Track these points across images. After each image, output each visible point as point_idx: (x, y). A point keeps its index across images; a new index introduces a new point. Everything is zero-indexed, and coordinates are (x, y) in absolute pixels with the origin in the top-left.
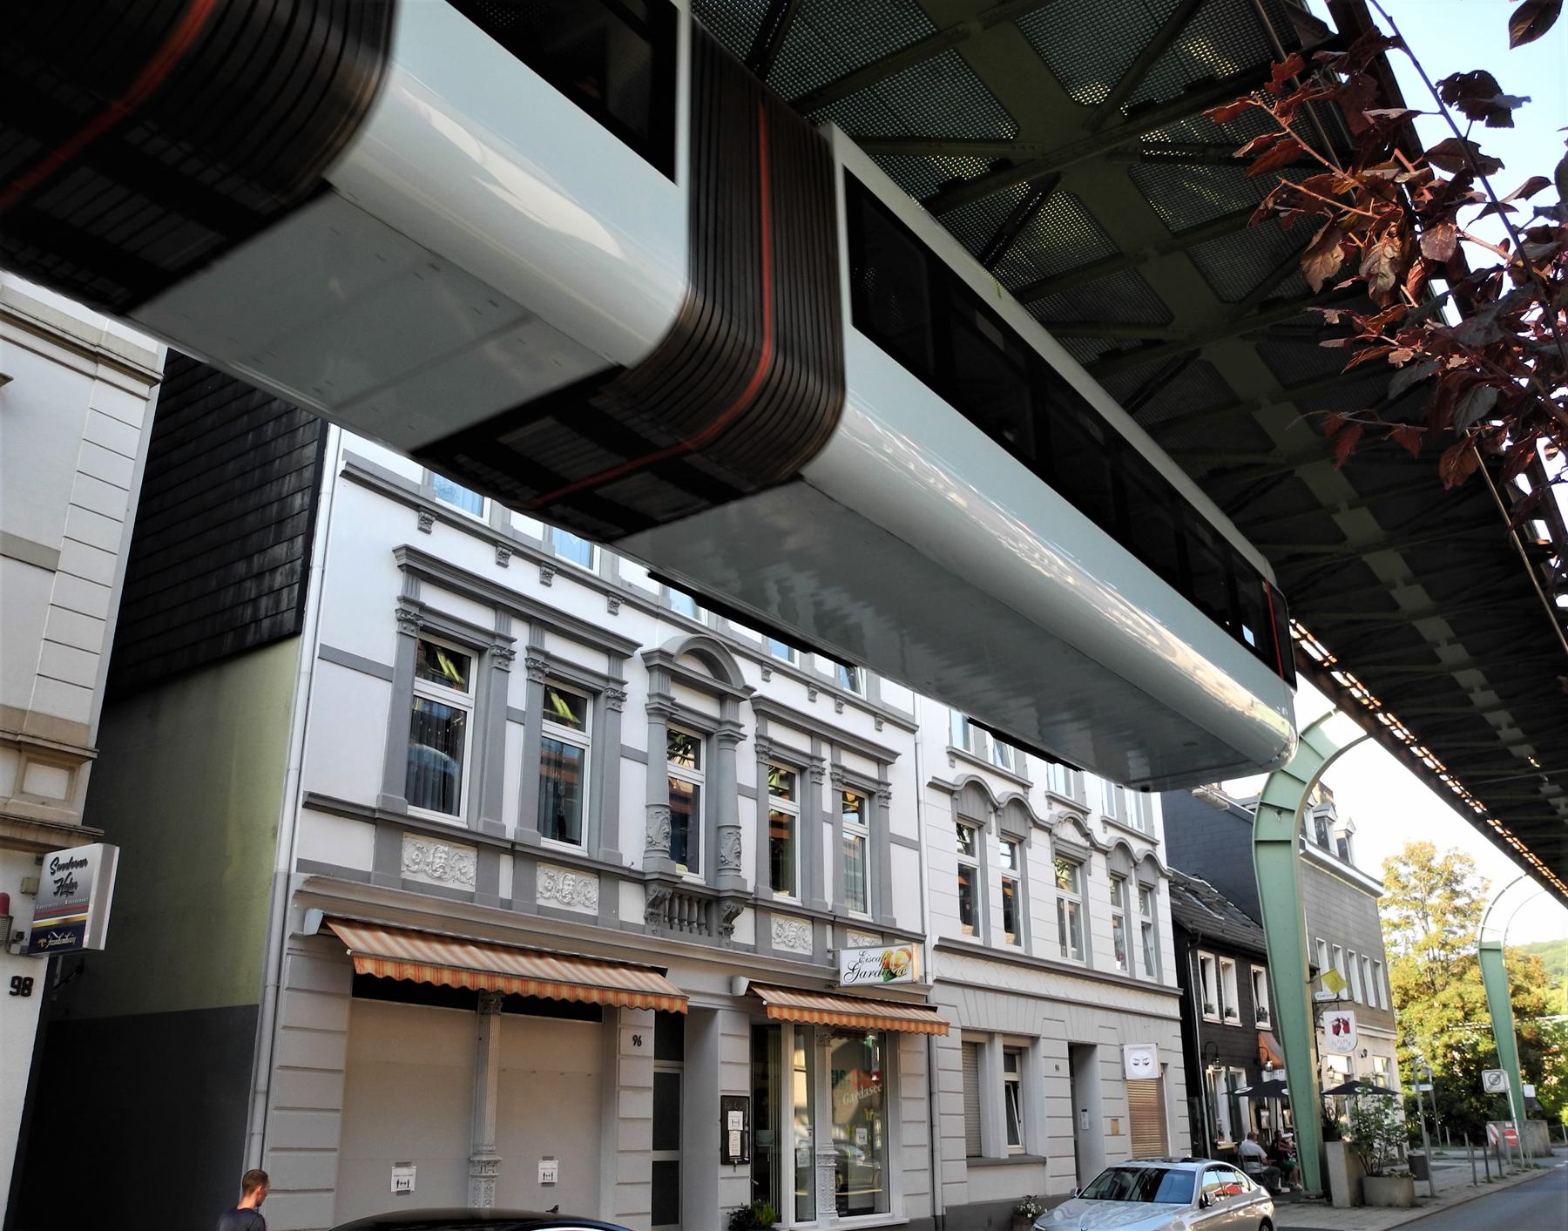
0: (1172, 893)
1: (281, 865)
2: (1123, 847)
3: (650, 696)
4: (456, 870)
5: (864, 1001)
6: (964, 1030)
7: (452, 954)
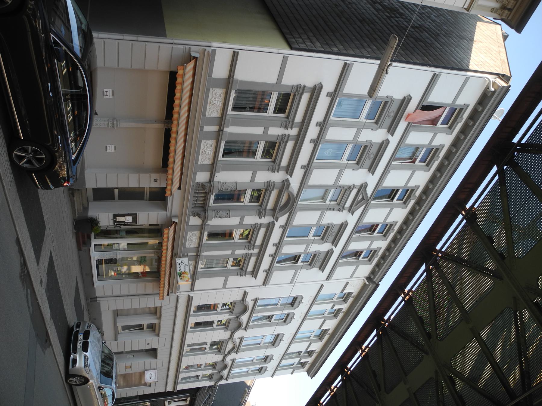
0: (210, 387)
1: (214, 44)
2: (225, 367)
3: (274, 182)
4: (213, 110)
6: (161, 307)
7: (185, 100)
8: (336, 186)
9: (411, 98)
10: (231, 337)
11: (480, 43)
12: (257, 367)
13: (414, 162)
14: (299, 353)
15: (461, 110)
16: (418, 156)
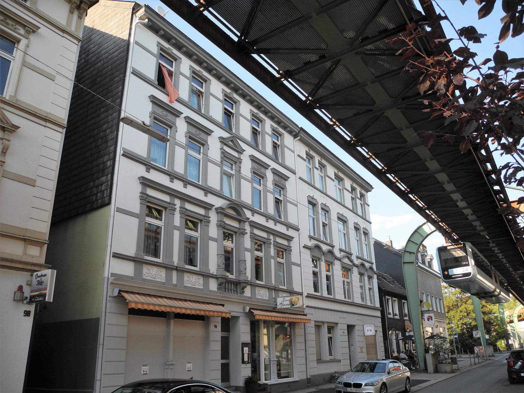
0: (378, 279)
1: (106, 275)
2: (362, 265)
5: (285, 313)
6: (315, 321)
8: (221, 165)
9: (152, 95)
10: (339, 260)
11: (95, 23)
12: (363, 236)
13: (201, 92)
14: (353, 199)
15: (162, 49)
16: (197, 88)
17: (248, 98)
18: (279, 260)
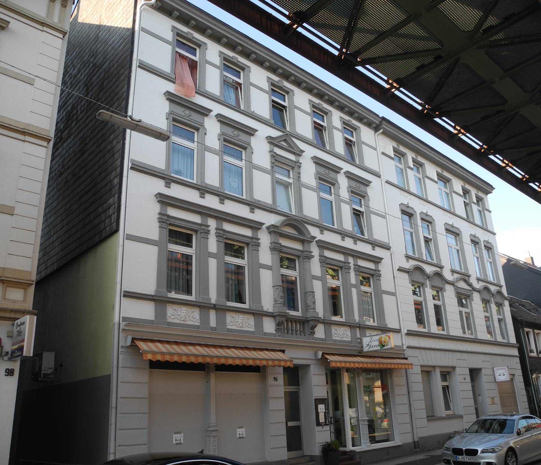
0: (511, 306)
1: (116, 319)
2: (486, 289)
3: (271, 243)
5: (375, 357)
6: (422, 366)
7: (181, 349)
8: (272, 172)
9: (167, 92)
10: (452, 284)
11: (102, 17)
12: (485, 252)
13: (240, 84)
14: (466, 205)
16: (233, 80)
17: (304, 85)
18: (364, 288)
